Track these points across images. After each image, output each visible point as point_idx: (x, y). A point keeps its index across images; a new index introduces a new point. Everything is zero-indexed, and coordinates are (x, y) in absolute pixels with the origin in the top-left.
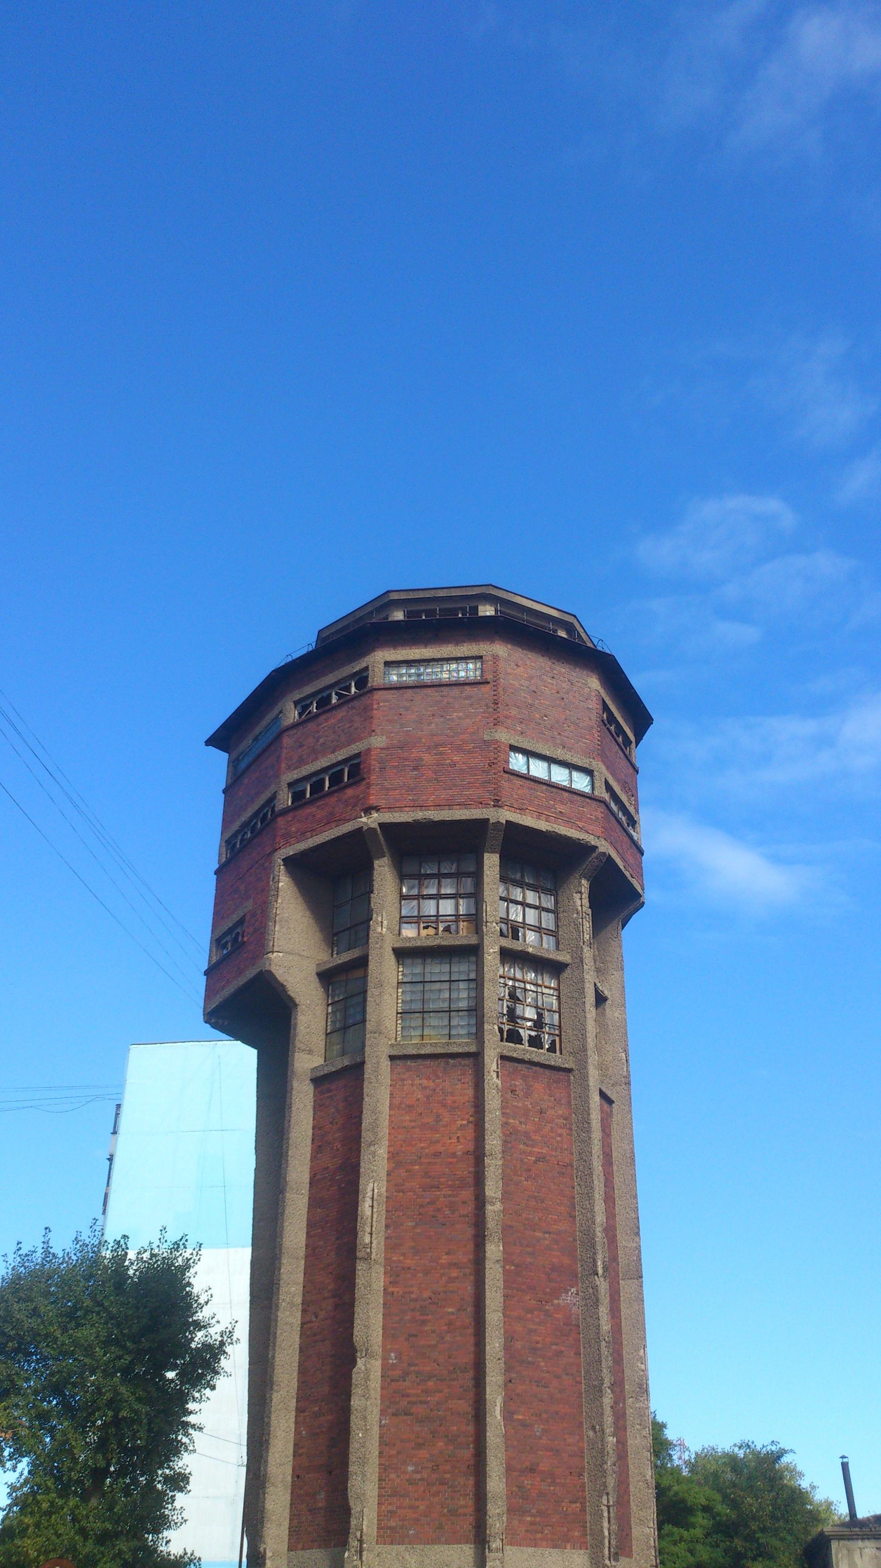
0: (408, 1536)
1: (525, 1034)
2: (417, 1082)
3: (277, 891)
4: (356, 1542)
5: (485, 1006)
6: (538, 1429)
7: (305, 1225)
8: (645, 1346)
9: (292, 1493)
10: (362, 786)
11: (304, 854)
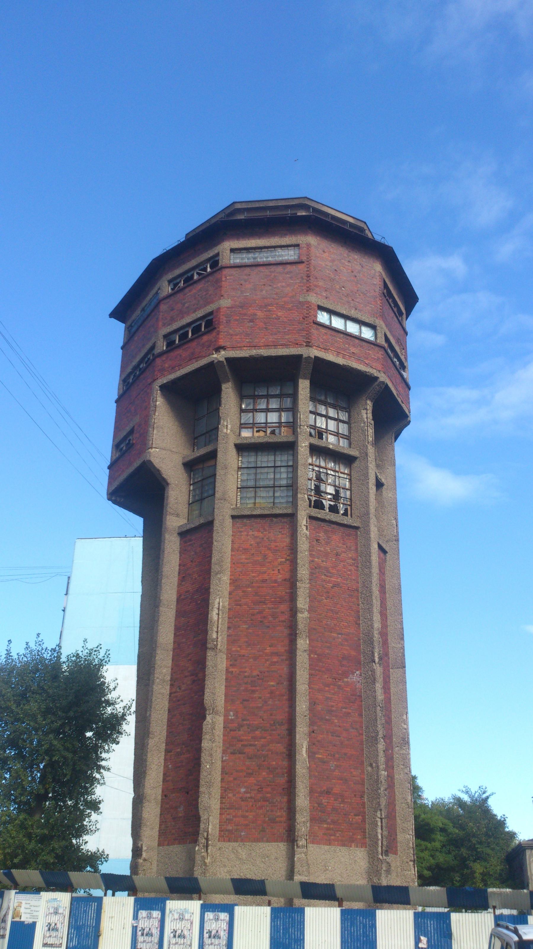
0: (241, 836)
1: (326, 503)
2: (251, 533)
3: (155, 408)
4: (204, 840)
5: (299, 482)
6: (332, 764)
7: (173, 629)
8: (407, 713)
9: (161, 806)
10: (214, 333)
11: (174, 382)
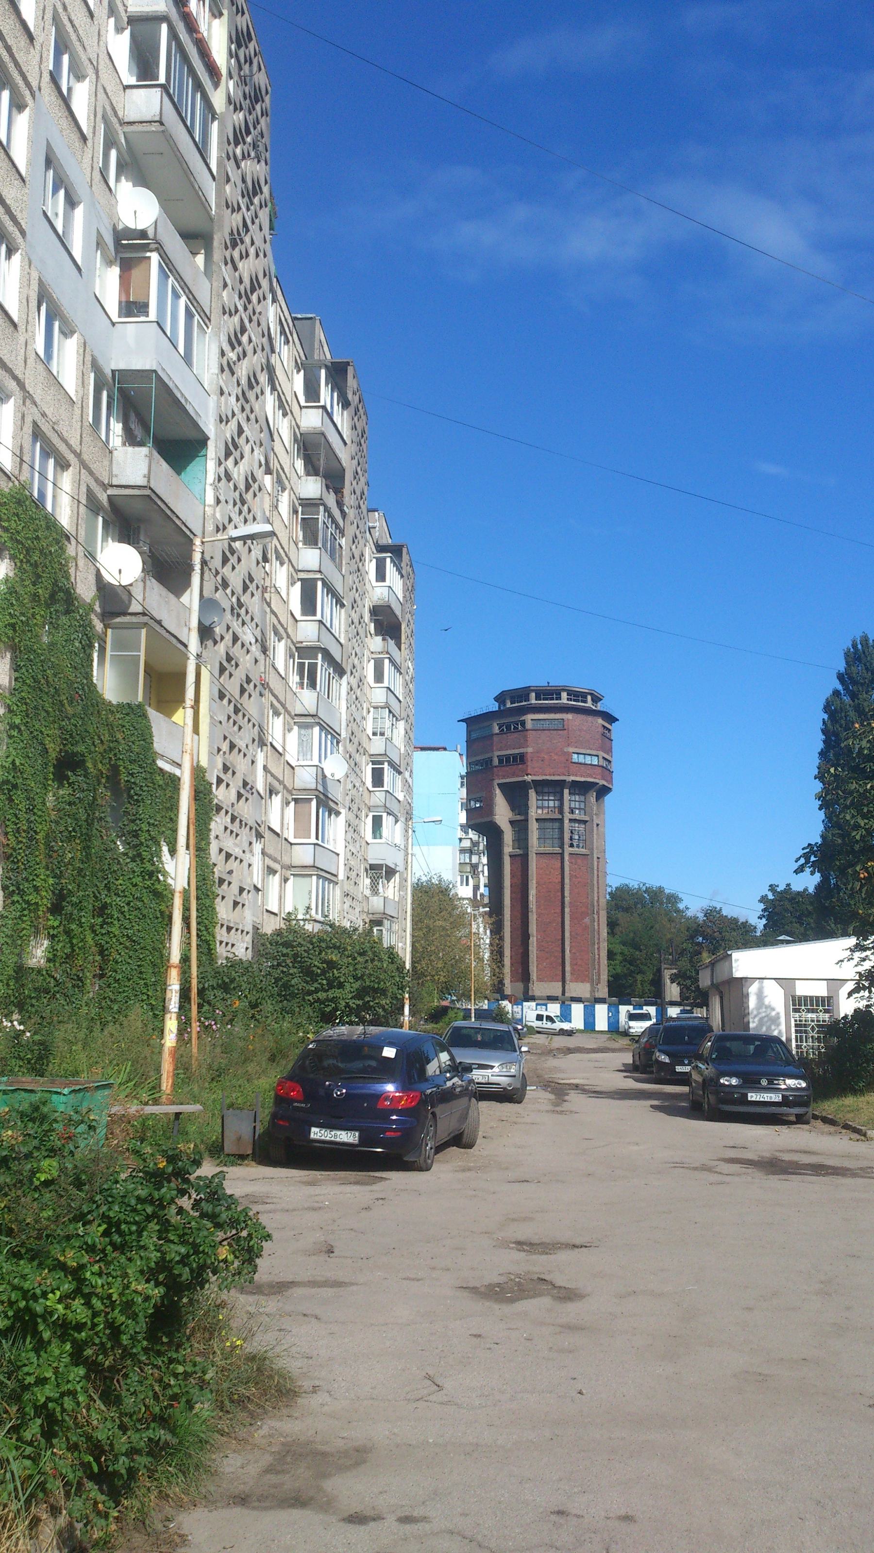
1: (575, 844)
